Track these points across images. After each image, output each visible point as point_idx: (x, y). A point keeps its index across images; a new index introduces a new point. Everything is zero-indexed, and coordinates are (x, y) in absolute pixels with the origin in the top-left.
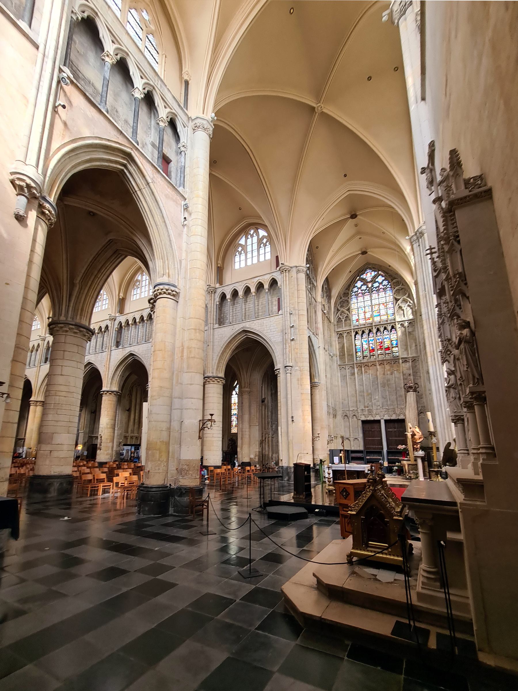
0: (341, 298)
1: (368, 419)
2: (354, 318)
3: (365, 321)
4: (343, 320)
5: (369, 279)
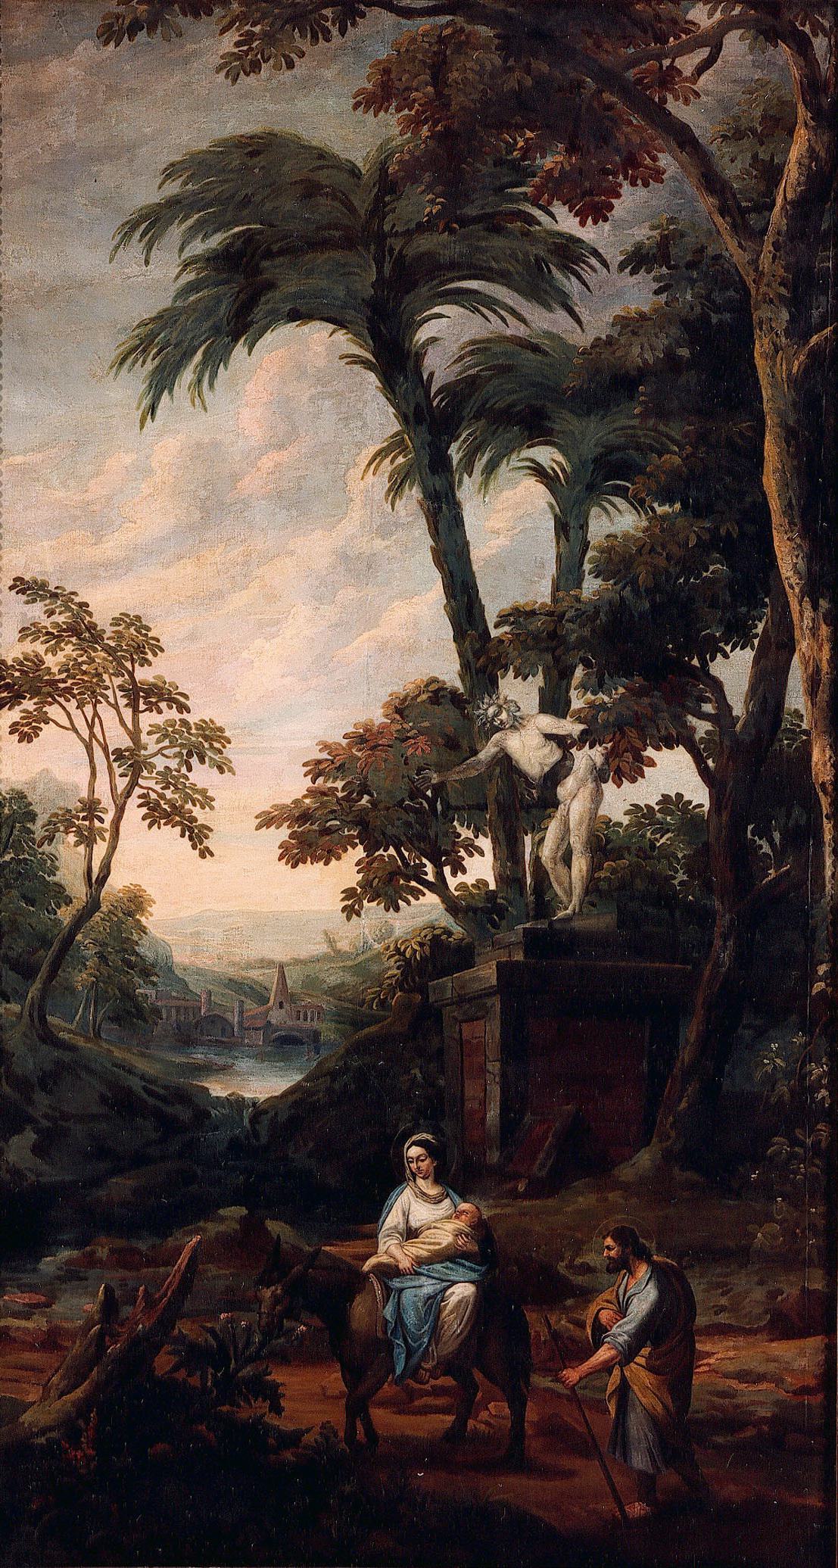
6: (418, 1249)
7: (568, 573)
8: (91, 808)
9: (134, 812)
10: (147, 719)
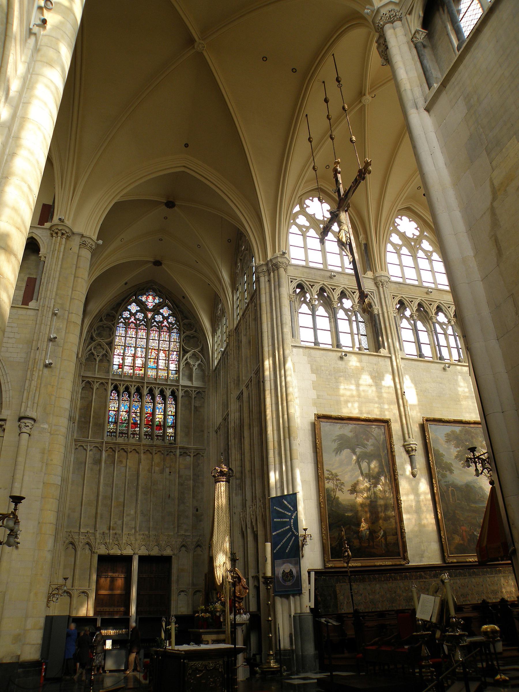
0: (101, 320)
1: (112, 552)
2: (117, 360)
3: (132, 371)
4: (98, 359)
5: (150, 306)
6: (364, 529)
7: (369, 471)
8: (334, 489)
9: (337, 490)
10: (338, 482)
